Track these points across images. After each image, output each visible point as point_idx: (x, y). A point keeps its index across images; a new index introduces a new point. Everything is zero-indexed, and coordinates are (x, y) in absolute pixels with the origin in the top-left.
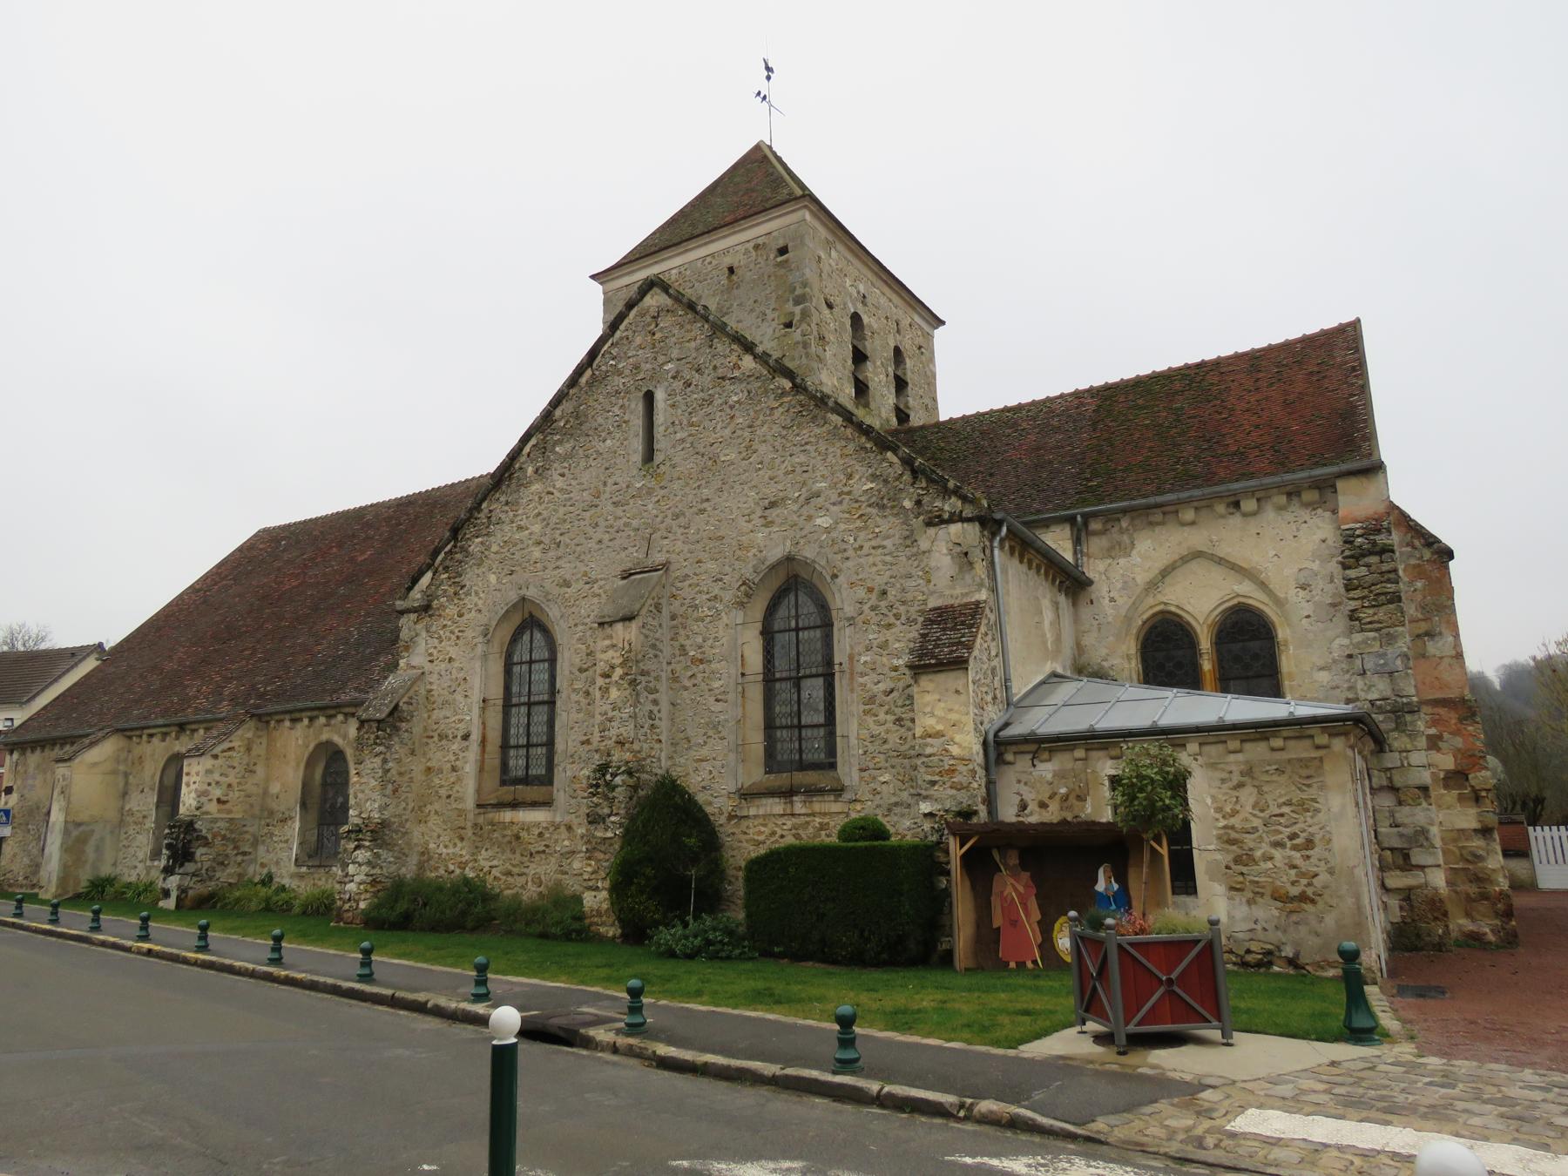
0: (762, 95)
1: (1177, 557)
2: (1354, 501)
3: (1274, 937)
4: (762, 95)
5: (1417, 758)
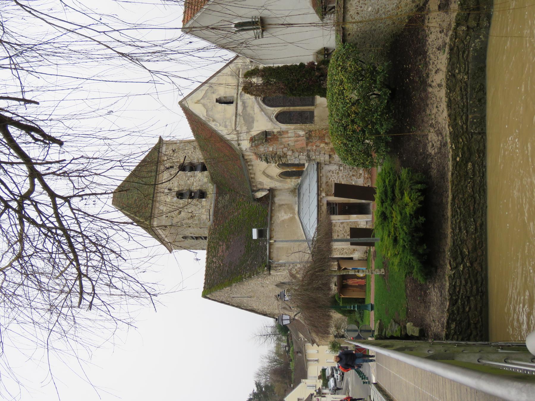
0: (94, 203)
1: (264, 176)
2: (250, 156)
3: (361, 252)
4: (94, 203)
5: (322, 159)
